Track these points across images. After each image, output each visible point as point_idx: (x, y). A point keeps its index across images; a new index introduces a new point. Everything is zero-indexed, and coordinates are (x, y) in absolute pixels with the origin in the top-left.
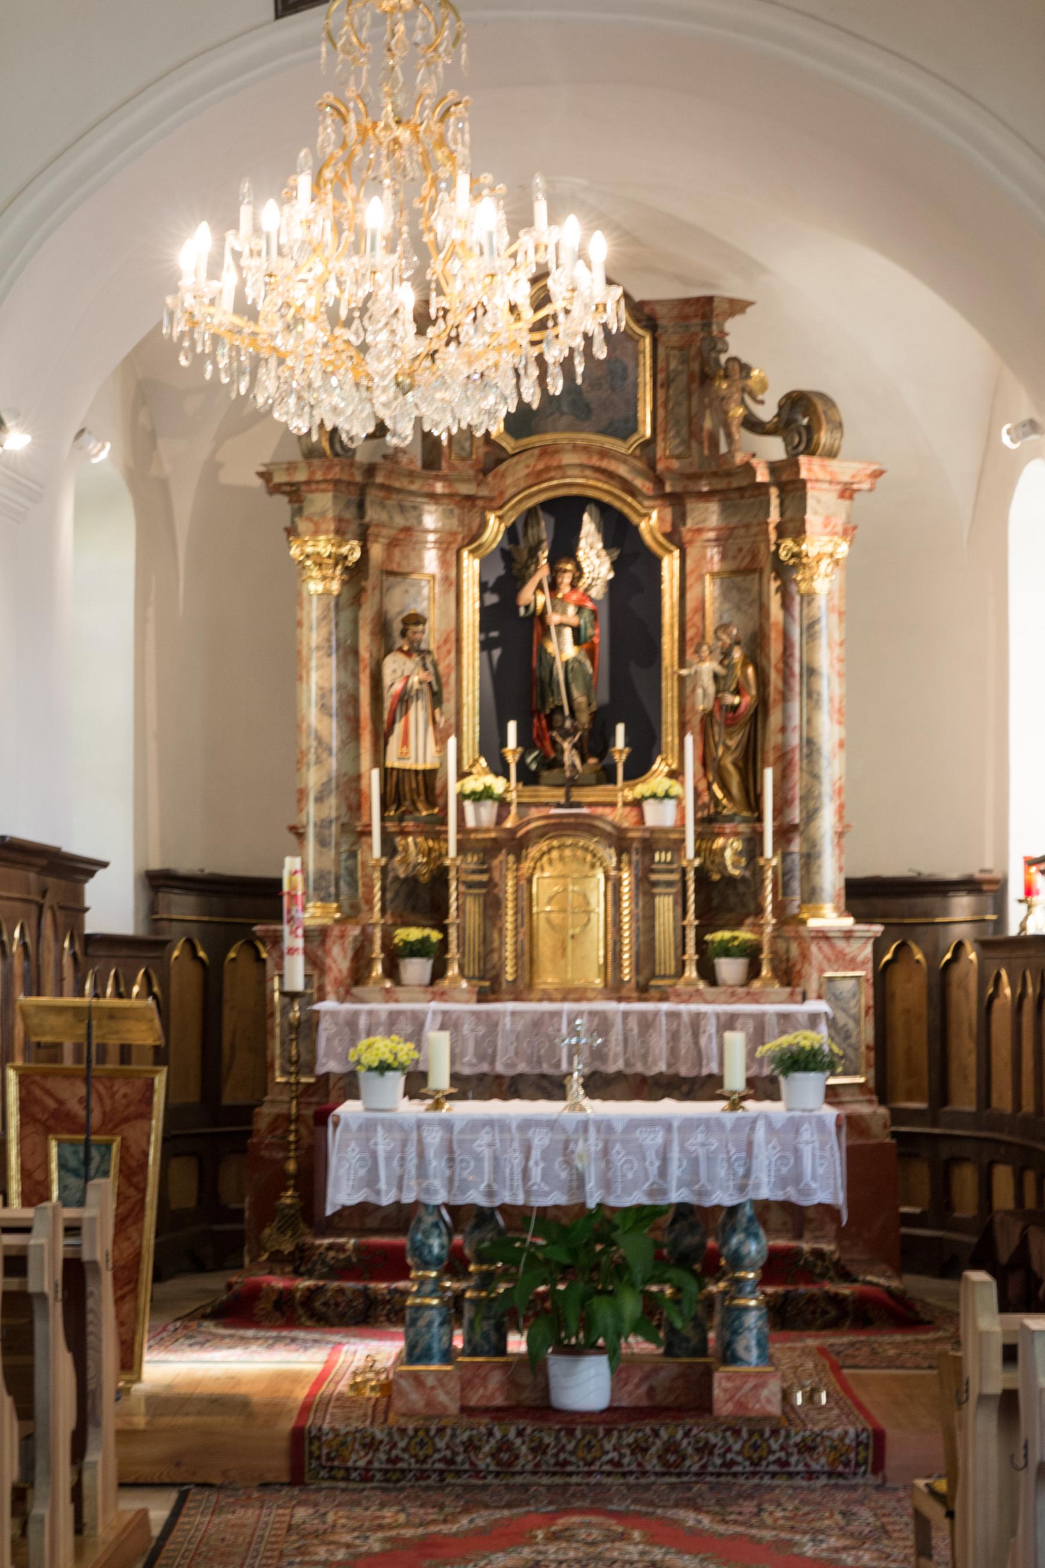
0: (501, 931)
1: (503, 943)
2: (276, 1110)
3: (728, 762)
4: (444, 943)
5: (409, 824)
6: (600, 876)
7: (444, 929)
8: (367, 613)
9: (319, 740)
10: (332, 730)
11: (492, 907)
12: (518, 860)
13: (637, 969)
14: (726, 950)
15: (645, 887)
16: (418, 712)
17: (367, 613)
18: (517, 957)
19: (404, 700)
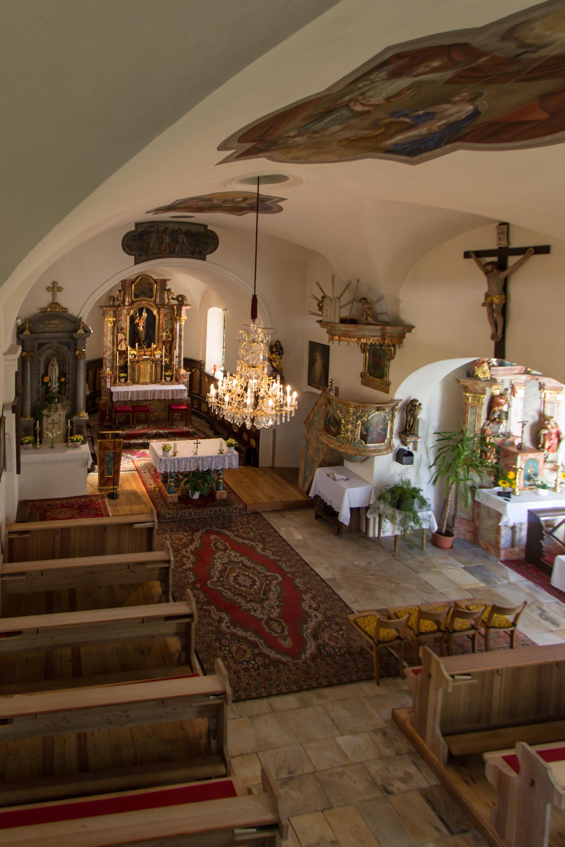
0: (135, 374)
1: (135, 376)
2: (103, 402)
3: (168, 348)
4: (127, 376)
5: (122, 359)
6: (149, 366)
7: (127, 375)
8: (116, 328)
9: (109, 347)
10: (111, 346)
11: (134, 370)
12: (138, 363)
13: (155, 378)
14: (168, 376)
15: (156, 367)
16: (123, 342)
17: (116, 328)
18: (138, 377)
19: (121, 341)
